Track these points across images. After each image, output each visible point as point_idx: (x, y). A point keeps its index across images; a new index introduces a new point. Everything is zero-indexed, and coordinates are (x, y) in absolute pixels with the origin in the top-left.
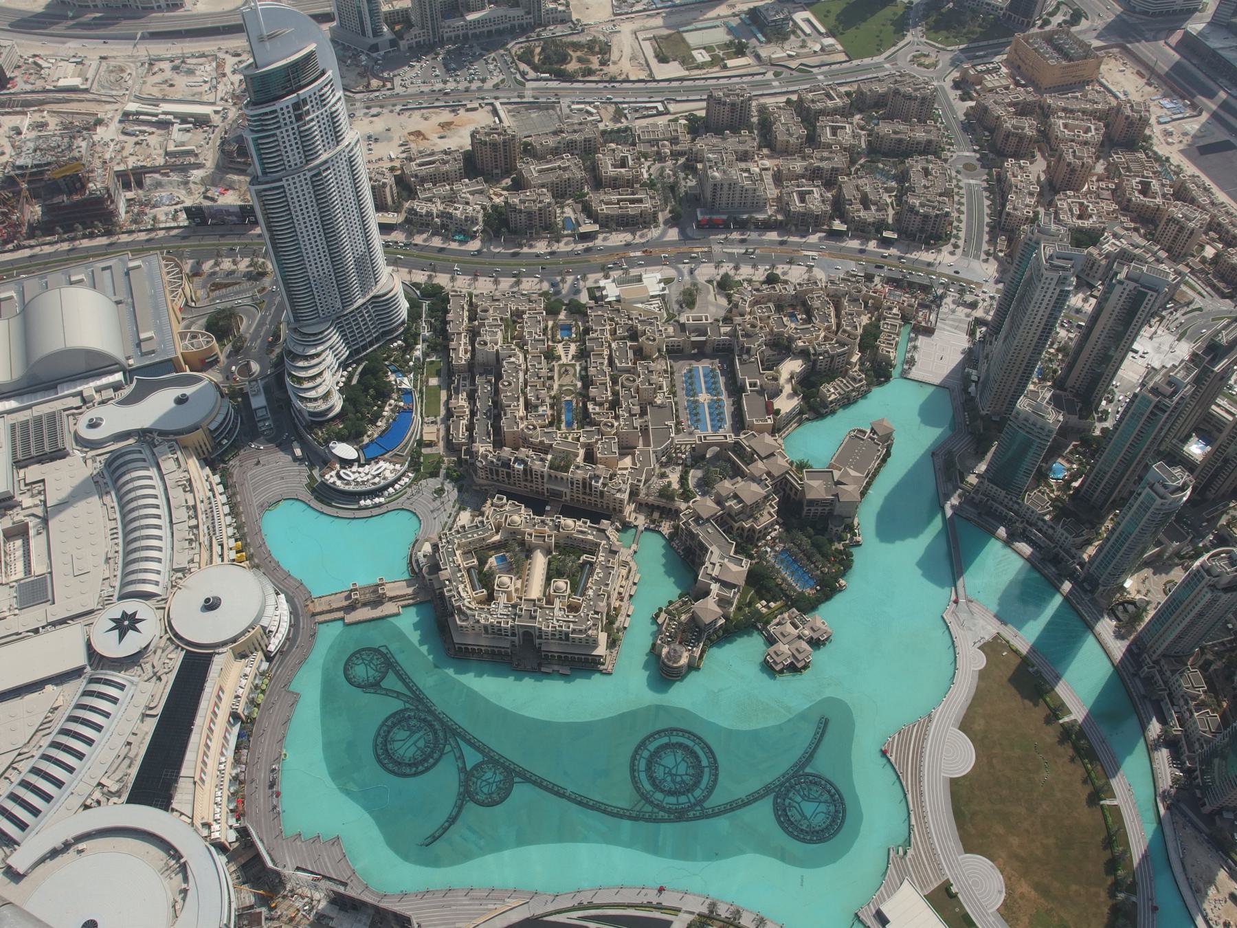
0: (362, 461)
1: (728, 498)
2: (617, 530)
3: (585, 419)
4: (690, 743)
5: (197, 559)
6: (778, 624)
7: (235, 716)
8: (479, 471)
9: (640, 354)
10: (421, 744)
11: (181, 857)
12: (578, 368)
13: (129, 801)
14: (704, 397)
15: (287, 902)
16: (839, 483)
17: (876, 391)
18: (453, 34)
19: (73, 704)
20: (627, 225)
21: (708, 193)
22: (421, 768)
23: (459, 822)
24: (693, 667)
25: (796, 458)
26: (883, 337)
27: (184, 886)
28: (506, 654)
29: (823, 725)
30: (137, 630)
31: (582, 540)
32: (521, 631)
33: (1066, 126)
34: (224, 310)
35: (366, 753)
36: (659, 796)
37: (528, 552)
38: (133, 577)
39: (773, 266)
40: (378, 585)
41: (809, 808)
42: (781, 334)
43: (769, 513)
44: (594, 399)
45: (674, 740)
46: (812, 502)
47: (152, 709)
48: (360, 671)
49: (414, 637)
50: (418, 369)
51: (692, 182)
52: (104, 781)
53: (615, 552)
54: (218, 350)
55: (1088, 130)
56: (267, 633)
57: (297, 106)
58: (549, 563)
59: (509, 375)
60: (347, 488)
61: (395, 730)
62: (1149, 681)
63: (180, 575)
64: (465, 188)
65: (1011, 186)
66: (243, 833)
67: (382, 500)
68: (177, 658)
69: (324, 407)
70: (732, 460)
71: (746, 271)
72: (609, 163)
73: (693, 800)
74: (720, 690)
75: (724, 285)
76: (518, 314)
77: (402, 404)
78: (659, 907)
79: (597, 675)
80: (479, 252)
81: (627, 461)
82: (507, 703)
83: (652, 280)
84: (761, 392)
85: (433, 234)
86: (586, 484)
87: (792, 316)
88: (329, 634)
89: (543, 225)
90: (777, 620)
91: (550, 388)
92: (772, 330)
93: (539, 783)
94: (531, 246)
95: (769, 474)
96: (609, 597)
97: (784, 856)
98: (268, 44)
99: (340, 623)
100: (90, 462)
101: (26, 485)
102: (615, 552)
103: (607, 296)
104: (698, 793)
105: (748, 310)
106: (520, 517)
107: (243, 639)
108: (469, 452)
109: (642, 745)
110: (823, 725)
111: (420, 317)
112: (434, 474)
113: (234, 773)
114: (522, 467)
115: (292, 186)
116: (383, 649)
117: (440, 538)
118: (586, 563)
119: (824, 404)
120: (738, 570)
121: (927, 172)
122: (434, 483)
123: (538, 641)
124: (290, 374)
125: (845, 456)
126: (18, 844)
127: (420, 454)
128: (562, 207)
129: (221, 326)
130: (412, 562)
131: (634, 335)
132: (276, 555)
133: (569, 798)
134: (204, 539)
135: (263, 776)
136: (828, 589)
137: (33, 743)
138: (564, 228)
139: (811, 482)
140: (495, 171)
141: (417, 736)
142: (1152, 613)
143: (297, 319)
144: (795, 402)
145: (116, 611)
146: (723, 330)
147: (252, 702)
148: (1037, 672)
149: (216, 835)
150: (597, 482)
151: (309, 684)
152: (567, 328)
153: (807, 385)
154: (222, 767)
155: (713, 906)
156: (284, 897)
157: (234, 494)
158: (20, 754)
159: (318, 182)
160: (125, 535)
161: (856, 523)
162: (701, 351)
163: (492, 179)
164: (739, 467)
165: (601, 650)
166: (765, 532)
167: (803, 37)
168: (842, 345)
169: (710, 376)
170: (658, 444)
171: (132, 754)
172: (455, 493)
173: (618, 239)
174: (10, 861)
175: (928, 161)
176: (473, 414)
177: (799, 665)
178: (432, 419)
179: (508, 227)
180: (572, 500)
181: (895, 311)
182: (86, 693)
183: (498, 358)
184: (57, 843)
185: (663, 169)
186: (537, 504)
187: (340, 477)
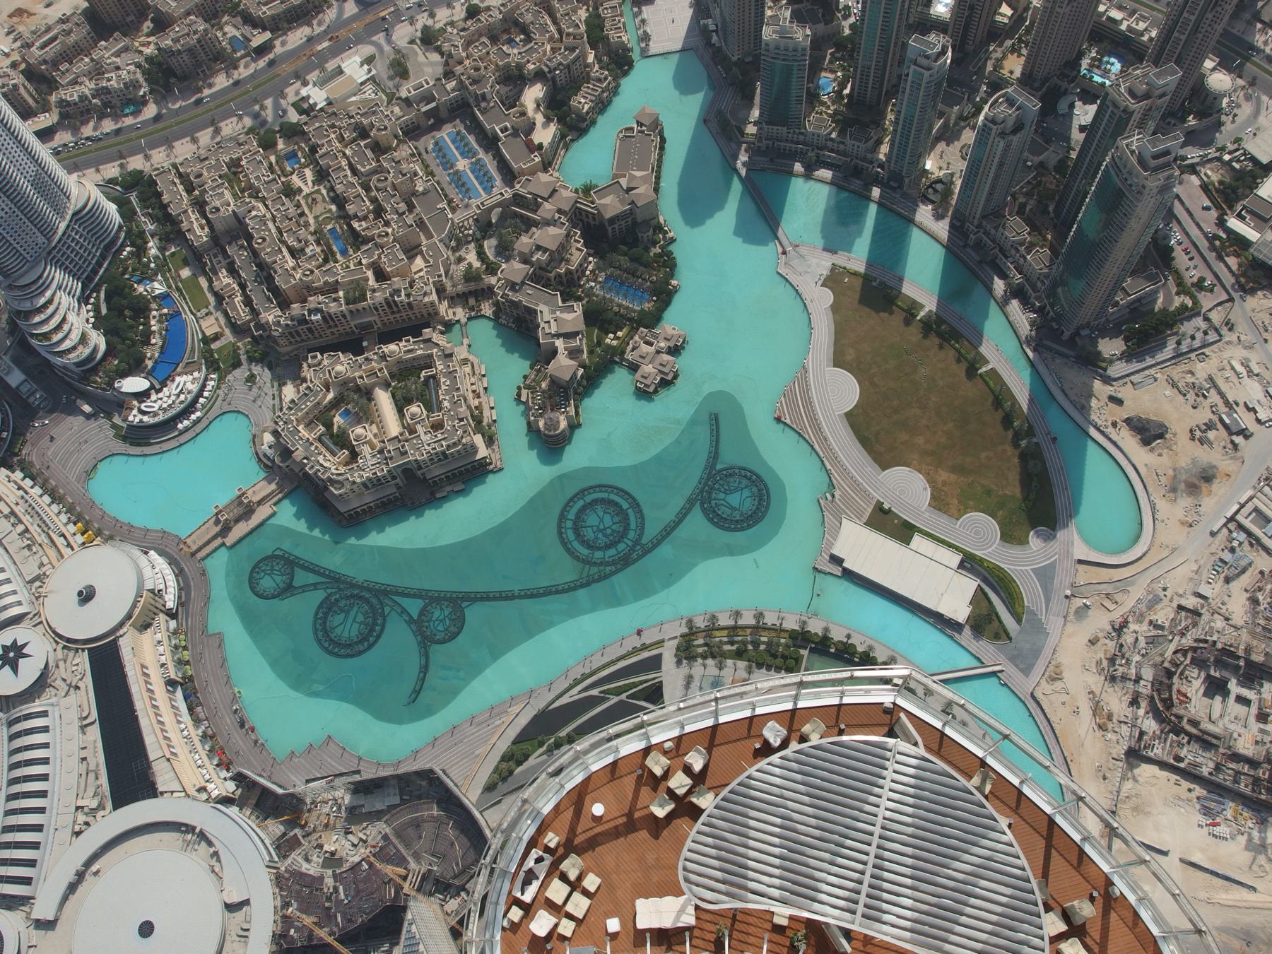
0: (158, 387)
1: (532, 254)
2: (442, 333)
3: (357, 240)
4: (604, 495)
5: (45, 560)
7: (171, 683)
8: (279, 340)
9: (379, 149)
10: (360, 618)
11: (194, 828)
12: (324, 192)
13: (115, 808)
14: (462, 164)
15: (315, 814)
16: (630, 189)
17: (627, 84)
22: (371, 639)
23: (432, 668)
24: (574, 426)
25: (578, 184)
26: (608, 24)
27: (212, 850)
28: (397, 499)
29: (715, 420)
30: (27, 656)
31: (414, 359)
35: (314, 651)
36: (598, 554)
37: (368, 394)
40: (240, 496)
41: (734, 499)
42: (508, 66)
43: (578, 249)
44: (356, 216)
45: (589, 498)
46: (612, 220)
47: (86, 718)
48: (267, 583)
49: (301, 526)
50: (162, 267)
52: (80, 803)
53: (451, 355)
56: (157, 594)
58: (393, 395)
59: (259, 231)
60: (156, 419)
61: (330, 618)
62: (979, 246)
63: (38, 584)
64: (106, 51)
66: (239, 778)
67: (198, 414)
68: (83, 660)
69: (87, 351)
70: (519, 214)
71: (443, 15)
73: (630, 543)
74: (609, 435)
75: (428, 39)
76: (235, 164)
77: (165, 311)
78: (645, 647)
79: (491, 477)
80: (157, 118)
81: (419, 262)
82: (420, 543)
83: (353, 66)
84: (515, 134)
85: (100, 118)
86: (390, 304)
87: (510, 42)
88: (218, 565)
89: (211, 58)
91: (307, 225)
92: (497, 65)
93: (486, 597)
94: (210, 86)
95: (560, 211)
96: (465, 400)
97: (731, 551)
99: (223, 549)
102: (451, 355)
103: (316, 104)
104: (631, 535)
105: (464, 54)
106: (343, 365)
108: (259, 326)
109: (562, 517)
110: (715, 420)
111: (136, 213)
112: (237, 365)
113: (200, 732)
114: (319, 316)
116: (278, 553)
117: (276, 423)
118: (428, 378)
119: (581, 118)
120: (573, 317)
122: (241, 373)
123: (419, 473)
124: (32, 335)
125: (623, 163)
126: (33, 898)
127: (211, 352)
128: (221, 29)
130: (261, 459)
131: (363, 133)
132: (124, 517)
133: (520, 597)
134: (42, 538)
135: (229, 721)
136: (664, 295)
138: (235, 51)
139: (603, 201)
140: (129, 19)
141: (352, 613)
142: (959, 183)
144: (553, 128)
146: (451, 85)
147: (180, 663)
148: (881, 283)
149: (215, 793)
150: (400, 296)
151: (224, 617)
152: (292, 156)
153: (556, 105)
154: (186, 733)
155: (690, 622)
156: (309, 811)
161: (662, 221)
162: (437, 120)
163: (129, 29)
164: (528, 218)
165: (483, 452)
166: (582, 268)
168: (573, 49)
169: (458, 139)
171: (92, 767)
172: (267, 374)
173: (297, 37)
174: (35, 916)
176: (243, 286)
177: (669, 378)
178: (204, 311)
179: (175, 76)
184: (70, 877)
186: (353, 345)
187: (144, 413)
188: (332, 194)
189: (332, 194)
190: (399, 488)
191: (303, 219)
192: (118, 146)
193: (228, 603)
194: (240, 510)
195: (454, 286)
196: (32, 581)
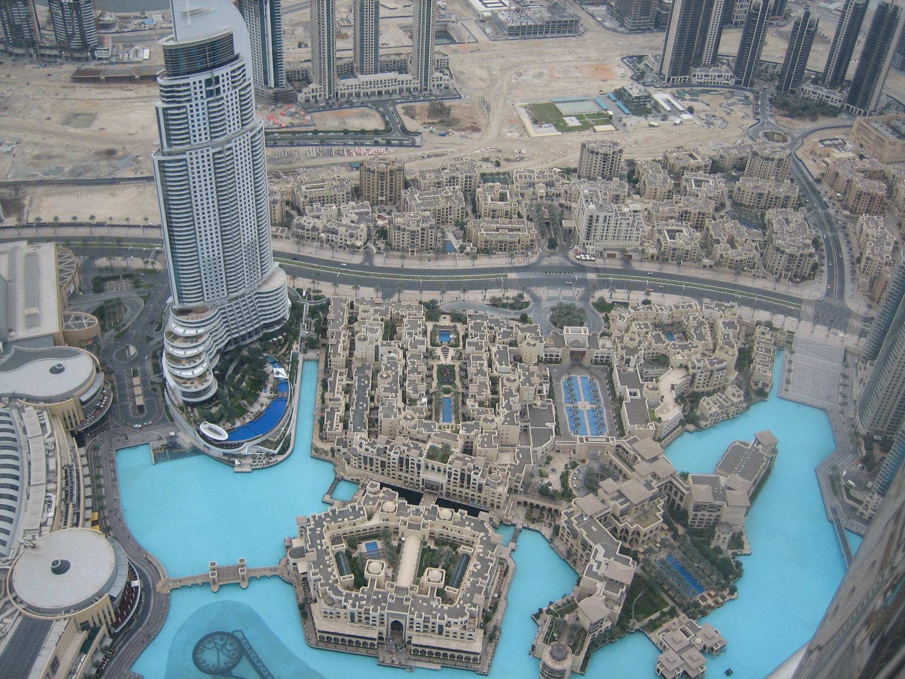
5: (50, 522)
14: (584, 405)
18: (347, 92)
26: (757, 359)
32: (392, 620)
34: (111, 300)
39: (648, 294)
40: (239, 566)
46: (697, 508)
48: (211, 657)
57: (209, 82)
64: (351, 210)
65: (867, 235)
69: (201, 388)
91: (429, 385)
98: (189, 21)
111: (302, 316)
114: (397, 456)
115: (194, 161)
117: (308, 520)
120: (625, 571)
139: (697, 486)
140: (380, 198)
168: (722, 361)
176: (347, 407)
180: (448, 494)
189: (463, 373)
190: (381, 638)
191: (429, 380)
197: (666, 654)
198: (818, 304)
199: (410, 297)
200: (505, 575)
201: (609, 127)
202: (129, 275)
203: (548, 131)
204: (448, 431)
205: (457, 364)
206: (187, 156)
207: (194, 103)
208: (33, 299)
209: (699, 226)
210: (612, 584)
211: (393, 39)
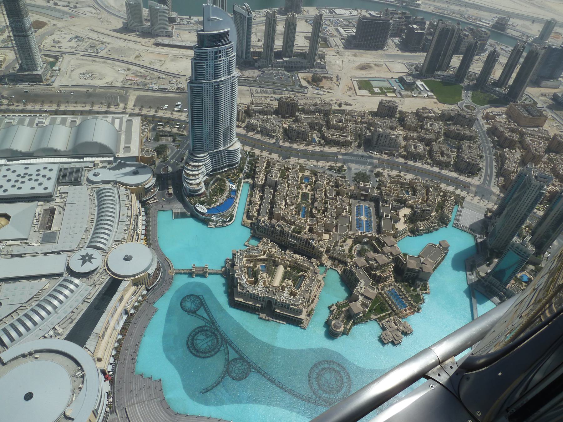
2: (318, 266)
5: (126, 238)
6: (387, 322)
9: (338, 193)
10: (210, 343)
14: (364, 218)
16: (423, 263)
19: (53, 289)
20: (339, 144)
21: (375, 137)
22: (207, 355)
24: (346, 333)
30: (91, 262)
31: (302, 266)
33: (531, 140)
34: (163, 145)
36: (320, 392)
37: (276, 265)
38: (96, 239)
39: (400, 172)
44: (316, 208)
46: (410, 270)
48: (188, 305)
51: (369, 134)
52: (57, 327)
53: (317, 273)
54: (156, 159)
55: (540, 144)
57: (216, 53)
63: (117, 243)
64: (273, 119)
68: (106, 279)
69: (196, 188)
71: (386, 172)
72: (335, 120)
79: (299, 328)
81: (326, 236)
85: (257, 133)
86: (307, 242)
90: (387, 320)
91: (297, 200)
92: (398, 195)
95: (391, 253)
96: (310, 293)
100: (90, 190)
101: (60, 193)
102: (317, 273)
106: (275, 250)
107: (138, 276)
115: (206, 88)
116: (201, 297)
118: (302, 275)
119: (418, 230)
120: (373, 293)
121: (470, 147)
124: (185, 172)
126: (7, 348)
129: (160, 150)
137: (29, 302)
139: (410, 260)
141: (209, 339)
143: (193, 150)
145: (84, 252)
157: (149, 217)
158: (21, 306)
159: (217, 91)
160: (97, 221)
163: (284, 117)
165: (303, 316)
167: (420, 90)
168: (430, 207)
169: (367, 209)
170: (341, 232)
171: (73, 318)
175: (470, 143)
176: (261, 205)
177: (396, 342)
181: (452, 198)
182: (60, 285)
183: (276, 183)
184: (26, 352)
185: (356, 128)
186: (284, 247)
188: (313, 197)
189: (313, 197)
192: (255, 144)
193: (169, 300)
194: (201, 273)
195: (333, 253)
196: (115, 241)
197: (385, 332)
198: (478, 186)
199: (293, 160)
200: (319, 287)
201: (394, 95)
202: (171, 135)
203: (365, 92)
204: (303, 221)
205: (311, 193)
206: (203, 85)
207: (208, 61)
208: (128, 140)
209: (427, 145)
210: (366, 297)
211: (301, 43)
